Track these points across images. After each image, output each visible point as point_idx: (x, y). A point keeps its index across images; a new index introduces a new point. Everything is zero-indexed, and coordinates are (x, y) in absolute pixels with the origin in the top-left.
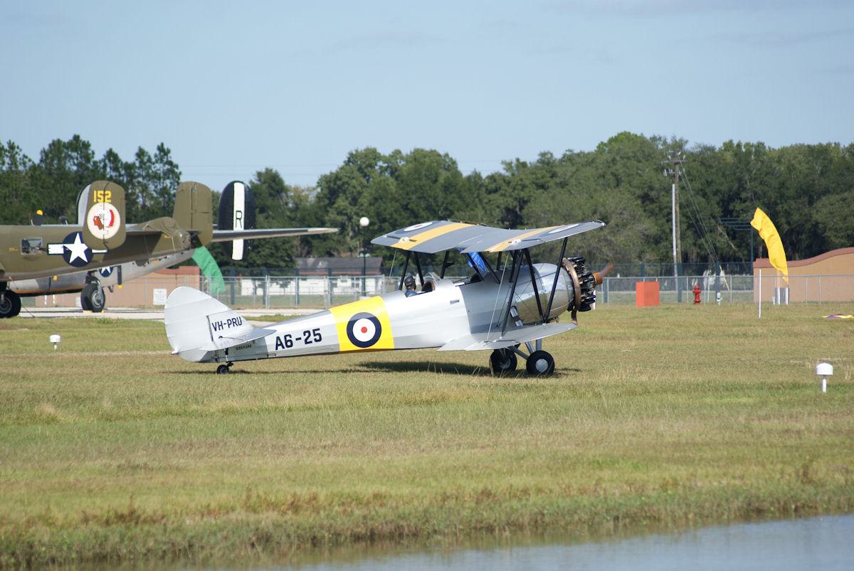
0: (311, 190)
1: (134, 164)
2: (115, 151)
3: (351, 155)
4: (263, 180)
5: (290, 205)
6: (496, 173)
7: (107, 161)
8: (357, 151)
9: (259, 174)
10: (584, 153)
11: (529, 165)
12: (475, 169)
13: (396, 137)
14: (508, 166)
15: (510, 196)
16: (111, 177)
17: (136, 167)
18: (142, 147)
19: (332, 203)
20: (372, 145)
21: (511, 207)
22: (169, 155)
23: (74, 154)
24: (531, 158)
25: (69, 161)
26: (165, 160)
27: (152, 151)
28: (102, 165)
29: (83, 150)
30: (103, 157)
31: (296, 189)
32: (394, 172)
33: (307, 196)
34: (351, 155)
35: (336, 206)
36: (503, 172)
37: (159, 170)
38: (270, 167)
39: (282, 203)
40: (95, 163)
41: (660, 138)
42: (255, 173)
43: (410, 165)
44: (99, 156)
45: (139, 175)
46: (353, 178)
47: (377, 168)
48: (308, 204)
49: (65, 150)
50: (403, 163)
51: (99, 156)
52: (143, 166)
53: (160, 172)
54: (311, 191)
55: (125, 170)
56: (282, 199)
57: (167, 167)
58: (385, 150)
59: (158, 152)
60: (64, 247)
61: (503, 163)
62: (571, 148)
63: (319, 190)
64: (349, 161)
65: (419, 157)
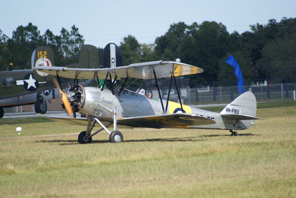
0: (151, 45)
1: (60, 36)
2: (50, 30)
4: (127, 41)
5: (142, 54)
6: (247, 32)
7: (47, 36)
8: (174, 24)
9: (125, 39)
10: (292, 19)
11: (264, 27)
12: (235, 30)
13: (194, 16)
14: (253, 28)
16: (49, 43)
17: (61, 38)
18: (64, 28)
19: (162, 52)
20: (182, 20)
21: (255, 49)
22: (78, 31)
23: (29, 33)
24: (265, 23)
25: (27, 36)
26: (76, 34)
28: (44, 38)
29: (34, 31)
31: (144, 45)
32: (194, 32)
33: (150, 49)
34: (171, 26)
35: (165, 53)
36: (251, 31)
37: (73, 39)
38: (130, 35)
39: (137, 53)
40: (40, 37)
42: (123, 38)
43: (202, 30)
44: (42, 33)
45: (63, 42)
46: (173, 38)
47: (185, 32)
48: (151, 53)
49: (25, 31)
51: (42, 33)
52: (65, 37)
53: (74, 40)
54: (152, 46)
55: (56, 40)
56: (137, 51)
57: (77, 37)
58: (189, 23)
59: (72, 30)
61: (250, 26)
62: (285, 17)
63: (156, 45)
64: (171, 29)
65: (206, 24)
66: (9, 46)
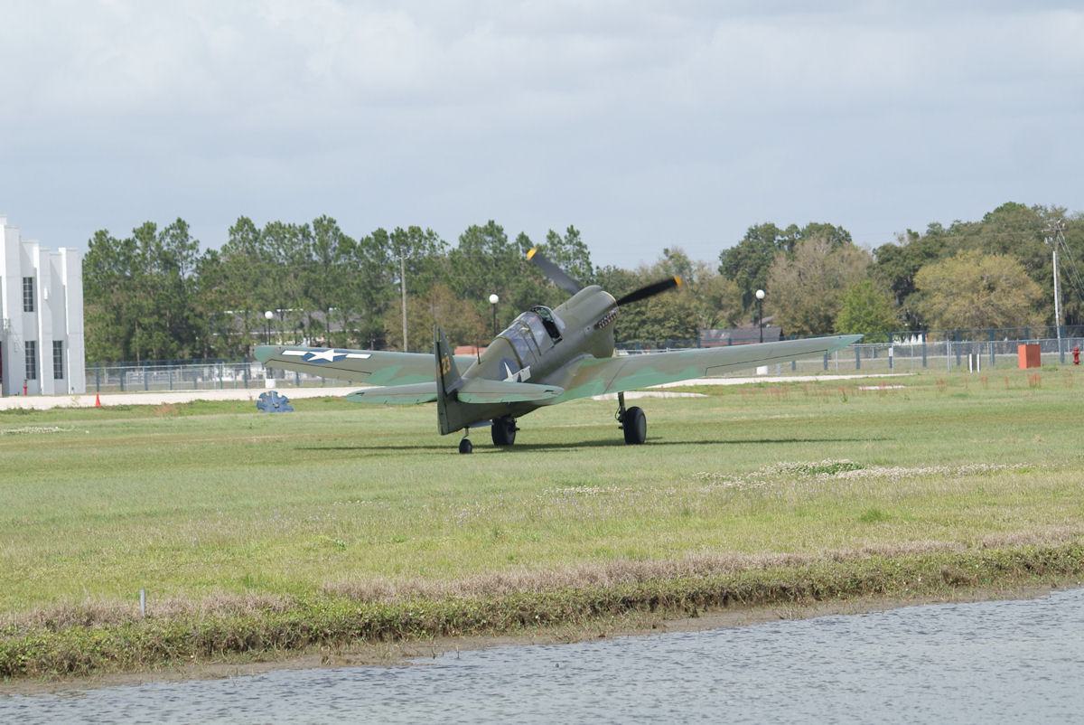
2: (526, 234)
3: (752, 230)
6: (889, 244)
8: (756, 226)
15: (902, 265)
20: (770, 221)
23: (489, 239)
27: (562, 233)
28: (515, 248)
34: (752, 230)
40: (509, 246)
41: (1041, 207)
44: (511, 240)
50: (799, 236)
59: (568, 234)
62: (959, 219)
64: (749, 237)
66: (453, 261)
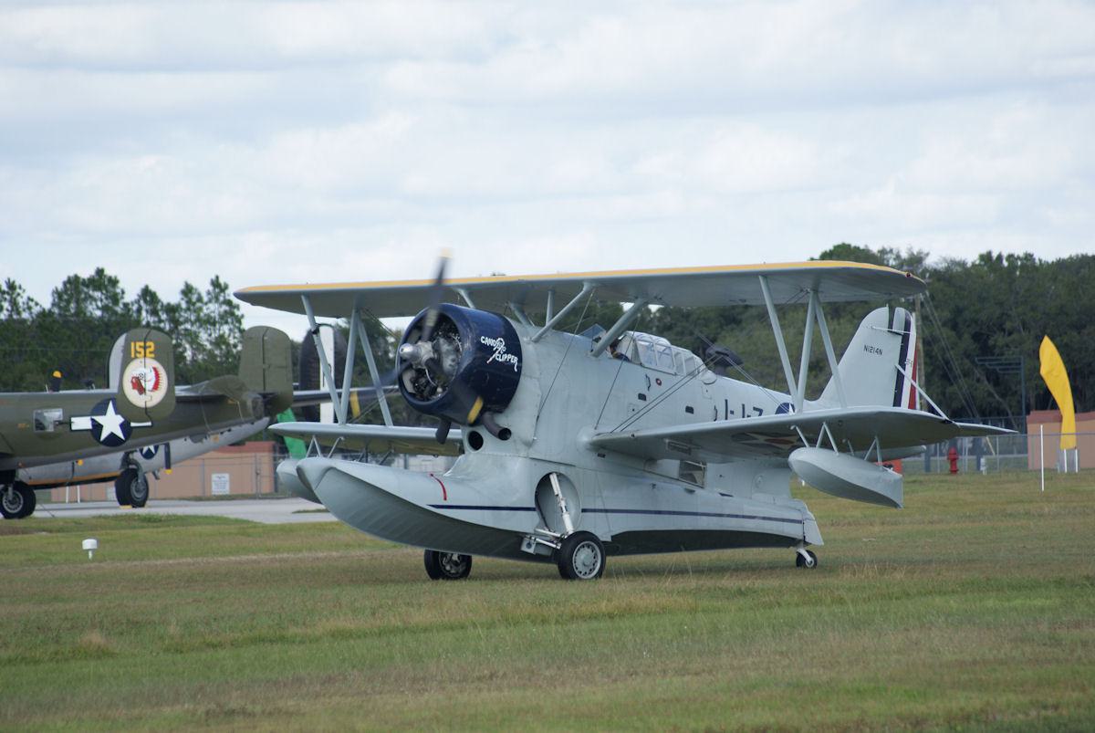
2: (152, 288)
7: (142, 302)
16: (148, 323)
17: (181, 309)
18: (189, 282)
22: (227, 292)
23: (97, 294)
25: (91, 304)
26: (221, 299)
27: (203, 287)
28: (135, 307)
29: (110, 288)
30: (136, 297)
37: (214, 312)
40: (126, 305)
44: (131, 294)
45: (187, 320)
49: (85, 290)
51: (131, 294)
52: (192, 308)
53: (216, 315)
55: (167, 315)
57: (225, 308)
59: (211, 288)
60: (93, 420)
